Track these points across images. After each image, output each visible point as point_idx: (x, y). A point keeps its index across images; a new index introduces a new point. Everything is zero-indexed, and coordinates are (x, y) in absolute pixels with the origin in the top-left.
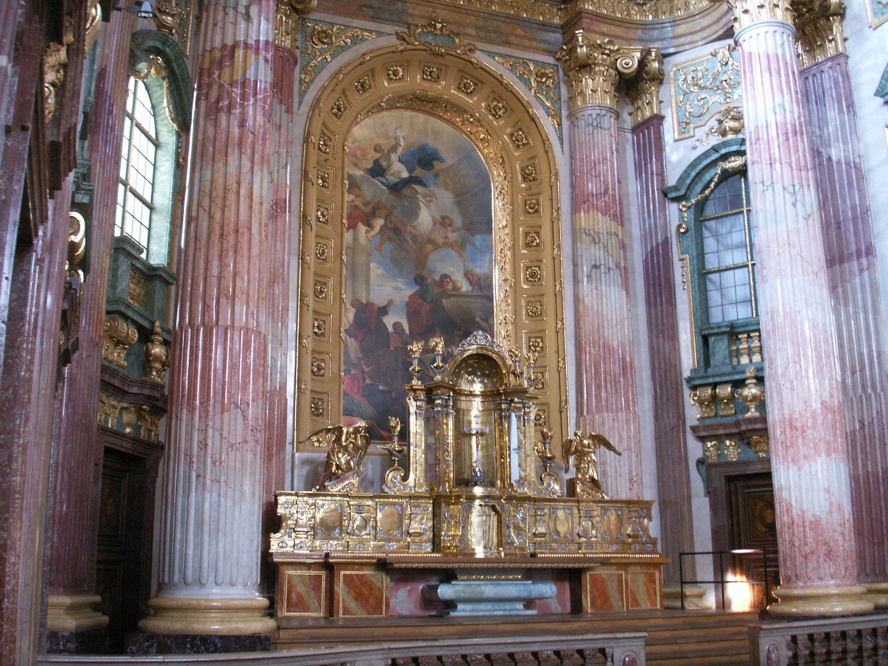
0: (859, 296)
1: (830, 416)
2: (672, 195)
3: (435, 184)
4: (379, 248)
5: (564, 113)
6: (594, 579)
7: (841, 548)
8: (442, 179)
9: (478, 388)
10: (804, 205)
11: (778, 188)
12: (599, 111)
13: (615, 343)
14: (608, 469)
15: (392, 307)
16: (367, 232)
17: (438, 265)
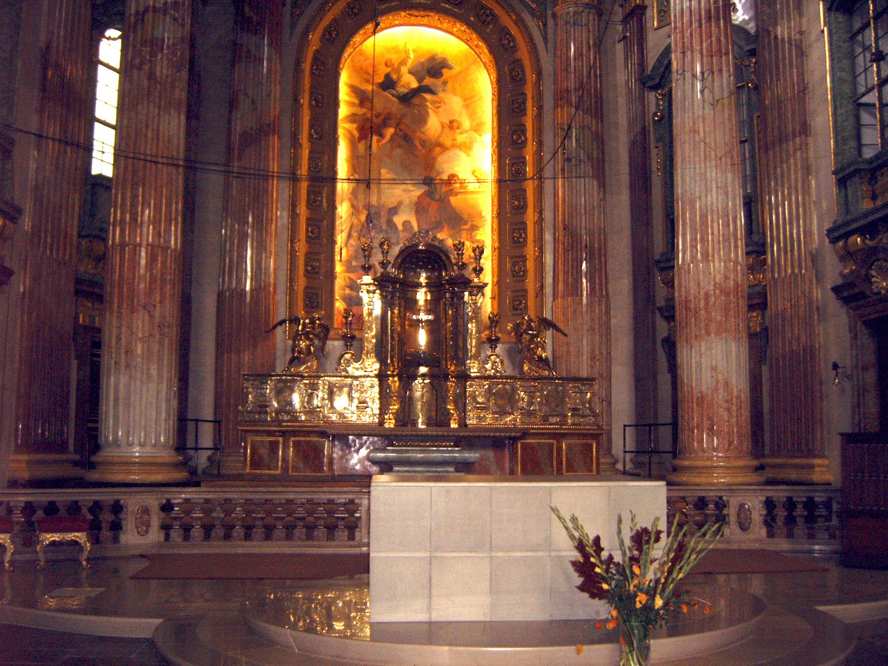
0: (793, 177)
1: (723, 298)
2: (650, 84)
3: (443, 91)
4: (389, 156)
5: (549, 12)
6: (525, 447)
7: (726, 424)
8: (450, 85)
9: (423, 279)
10: (712, 92)
11: (688, 75)
12: (576, 9)
14: (572, 349)
15: (402, 208)
16: (378, 141)
17: (445, 166)
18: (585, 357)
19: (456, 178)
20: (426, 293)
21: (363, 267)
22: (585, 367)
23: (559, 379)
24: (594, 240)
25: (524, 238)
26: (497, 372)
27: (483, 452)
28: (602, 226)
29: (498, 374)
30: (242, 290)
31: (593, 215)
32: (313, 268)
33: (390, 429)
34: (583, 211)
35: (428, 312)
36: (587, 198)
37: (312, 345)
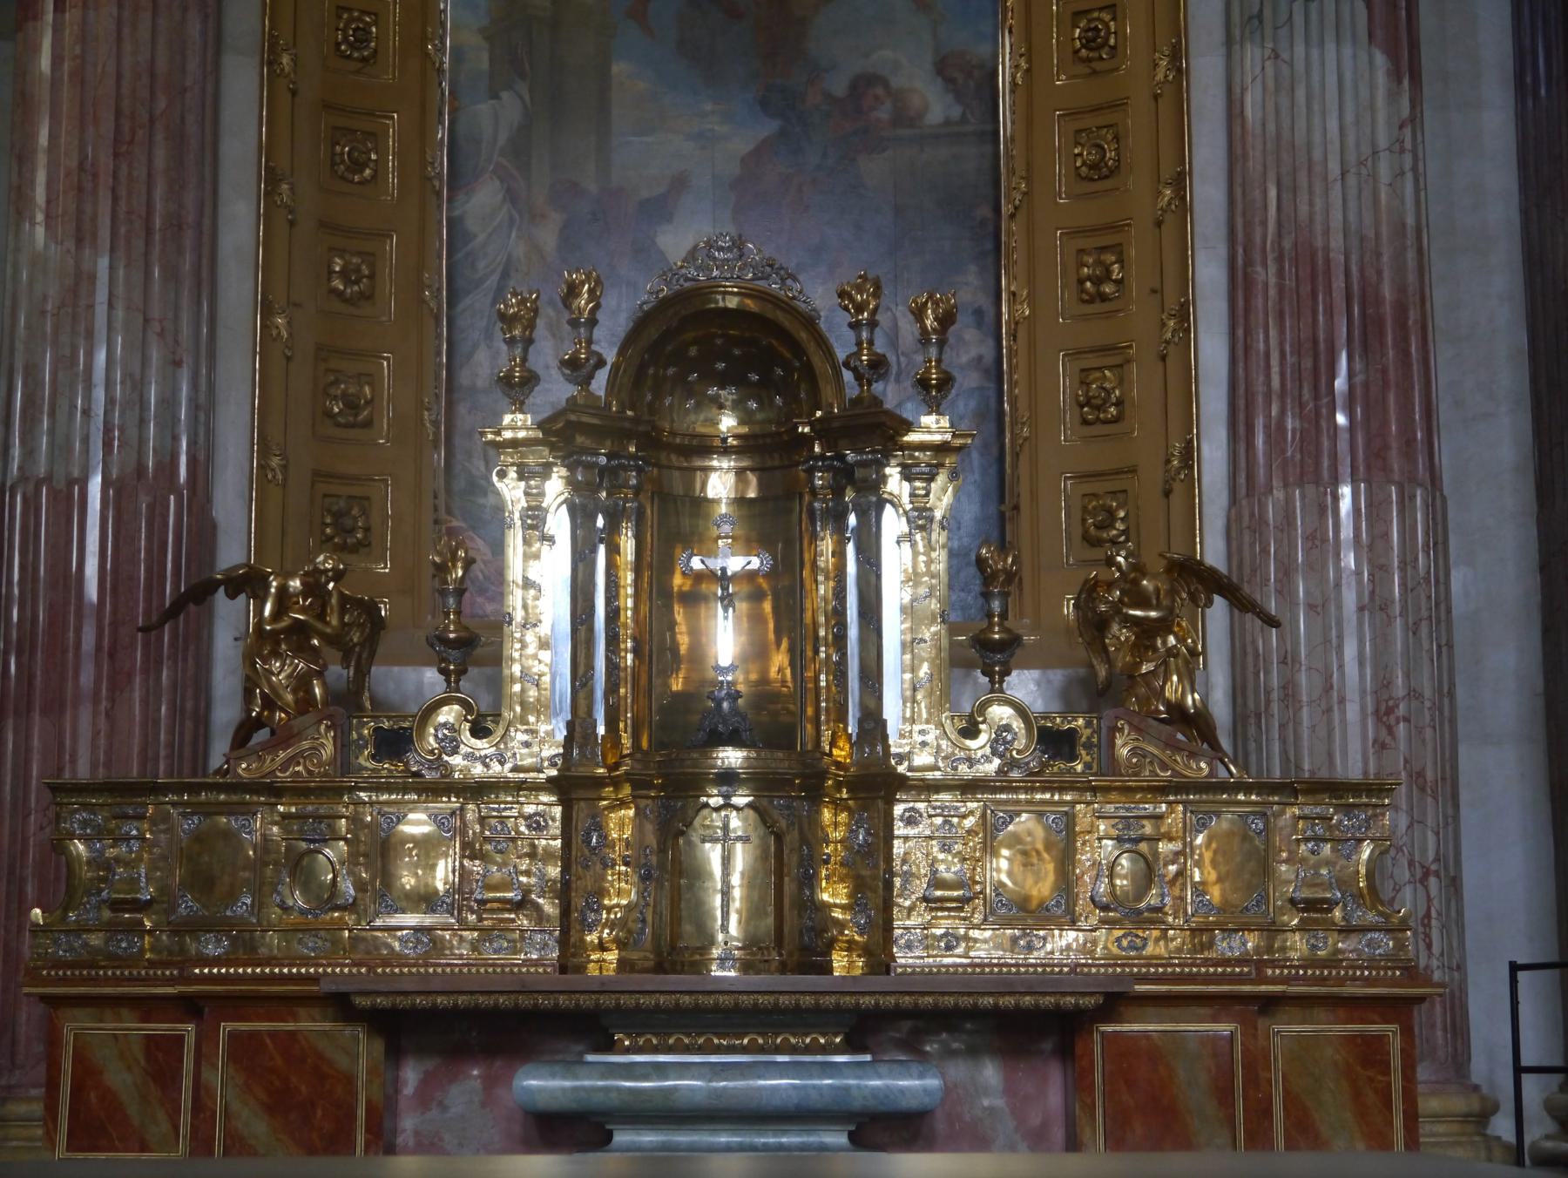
13: (1337, 242)
14: (1303, 679)
18: (1352, 711)
19: (880, 91)
20: (740, 473)
21: (506, 382)
22: (1355, 746)
23: (1248, 788)
24: (1379, 273)
25: (1119, 282)
26: (1012, 764)
27: (959, 1070)
28: (1410, 221)
29: (1015, 774)
30: (71, 483)
31: (1374, 176)
32: (352, 405)
33: (603, 987)
34: (1334, 168)
35: (748, 545)
36: (1349, 118)
37: (320, 675)
